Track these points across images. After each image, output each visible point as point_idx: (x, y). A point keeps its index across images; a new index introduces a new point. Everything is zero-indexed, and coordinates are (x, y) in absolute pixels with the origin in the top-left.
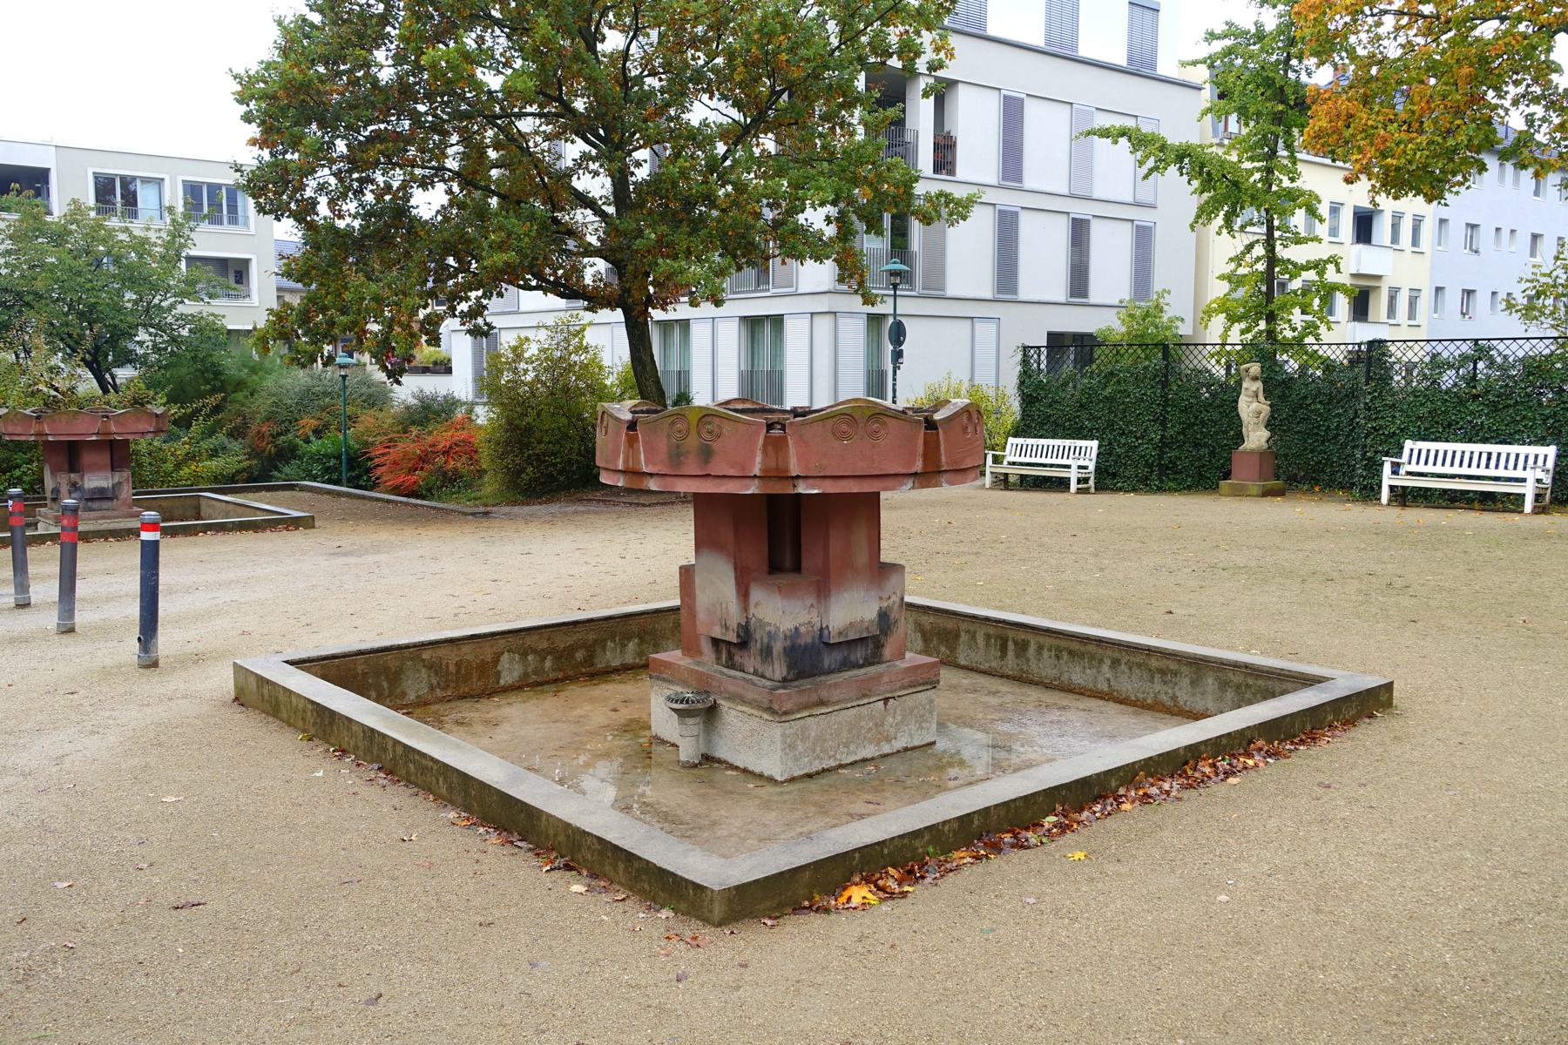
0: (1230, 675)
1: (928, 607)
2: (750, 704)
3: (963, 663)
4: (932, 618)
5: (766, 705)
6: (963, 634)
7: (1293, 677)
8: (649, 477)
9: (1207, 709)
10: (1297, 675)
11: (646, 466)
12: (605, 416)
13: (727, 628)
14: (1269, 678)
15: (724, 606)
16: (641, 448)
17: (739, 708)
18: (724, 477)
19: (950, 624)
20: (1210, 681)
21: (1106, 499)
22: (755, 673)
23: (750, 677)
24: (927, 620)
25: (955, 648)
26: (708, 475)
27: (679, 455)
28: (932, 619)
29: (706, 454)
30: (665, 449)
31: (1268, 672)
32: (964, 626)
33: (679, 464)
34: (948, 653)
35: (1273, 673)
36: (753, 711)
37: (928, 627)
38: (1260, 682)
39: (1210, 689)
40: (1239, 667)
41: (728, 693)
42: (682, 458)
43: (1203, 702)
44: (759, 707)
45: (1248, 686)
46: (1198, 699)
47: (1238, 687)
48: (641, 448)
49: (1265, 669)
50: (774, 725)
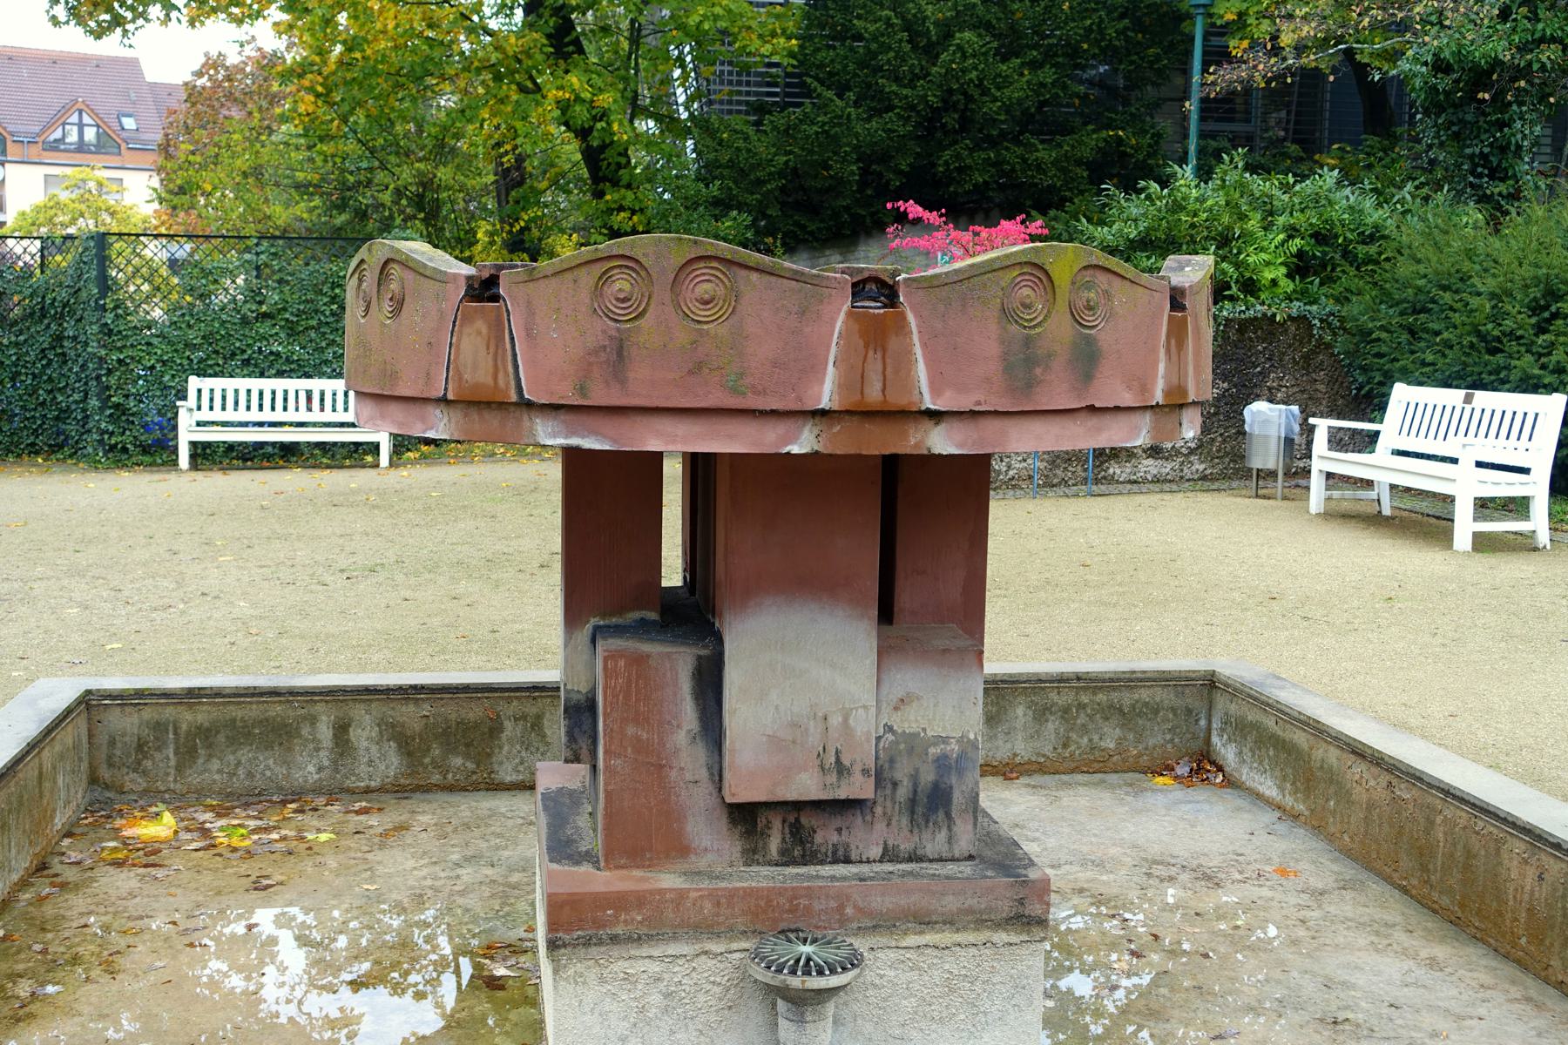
0: (1054, 696)
1: (414, 687)
2: (952, 923)
3: (509, 778)
4: (427, 706)
5: (1005, 908)
6: (508, 724)
7: (1149, 680)
8: (927, 424)
9: (1015, 755)
10: (1157, 675)
11: (936, 391)
12: (395, 270)
13: (841, 770)
14: (1114, 689)
15: (836, 720)
16: (918, 351)
17: (912, 940)
18: (1117, 409)
19: (474, 712)
20: (1020, 711)
21: (199, 475)
22: (889, 855)
23: (878, 867)
24: (411, 715)
25: (489, 755)
26: (1091, 409)
27: (1030, 362)
28: (426, 709)
29: (1087, 358)
30: (993, 349)
31: (1111, 680)
32: (510, 709)
33: (1030, 385)
34: (471, 766)
35: (1119, 680)
36: (958, 938)
37: (417, 726)
38: (1101, 697)
39: (1019, 724)
40: (1067, 680)
41: (870, 914)
42: (1038, 371)
43: (1009, 745)
44: (981, 920)
45: (1081, 706)
46: (1000, 743)
47: (1066, 710)
48: (918, 351)
49: (1107, 676)
50: (1024, 951)
